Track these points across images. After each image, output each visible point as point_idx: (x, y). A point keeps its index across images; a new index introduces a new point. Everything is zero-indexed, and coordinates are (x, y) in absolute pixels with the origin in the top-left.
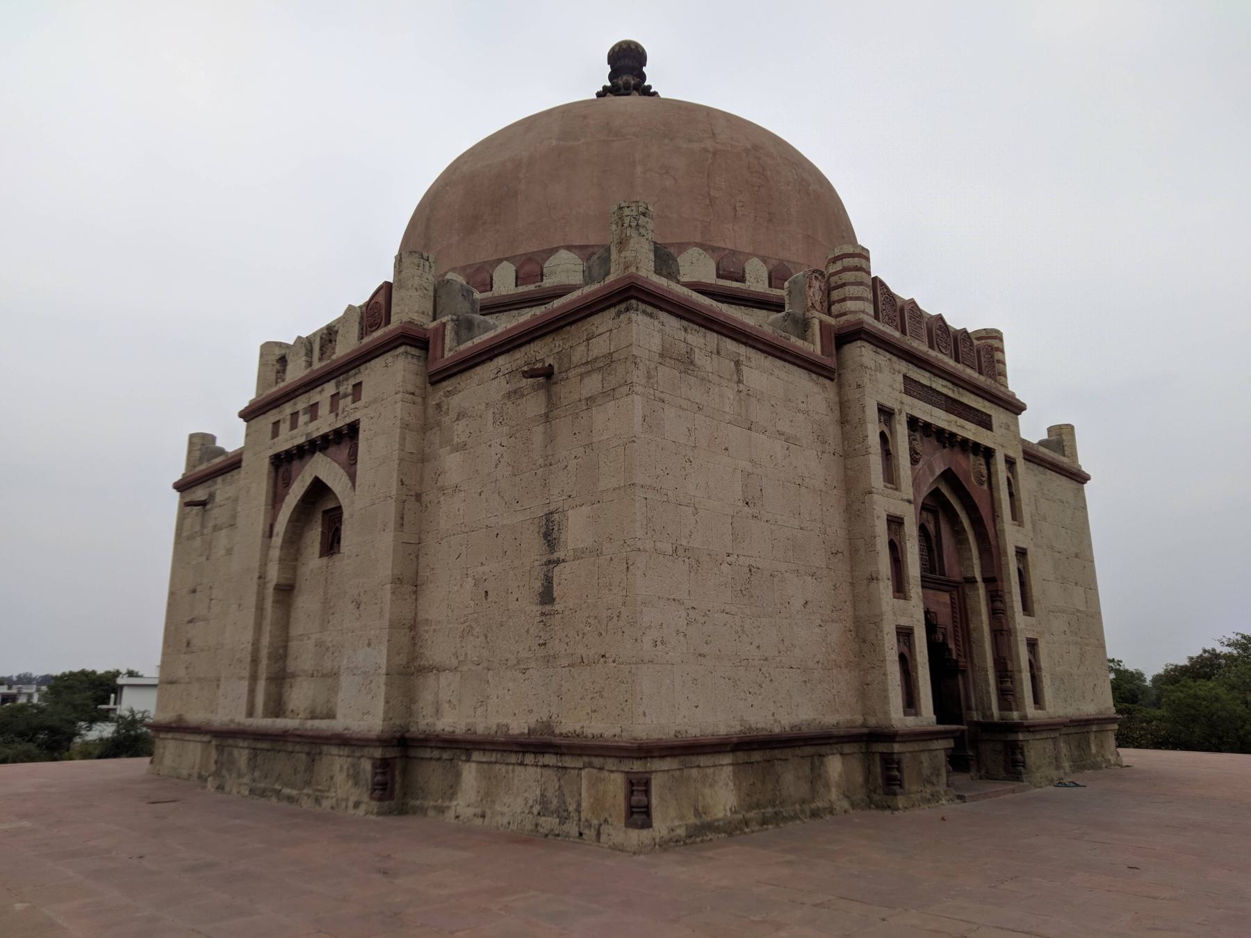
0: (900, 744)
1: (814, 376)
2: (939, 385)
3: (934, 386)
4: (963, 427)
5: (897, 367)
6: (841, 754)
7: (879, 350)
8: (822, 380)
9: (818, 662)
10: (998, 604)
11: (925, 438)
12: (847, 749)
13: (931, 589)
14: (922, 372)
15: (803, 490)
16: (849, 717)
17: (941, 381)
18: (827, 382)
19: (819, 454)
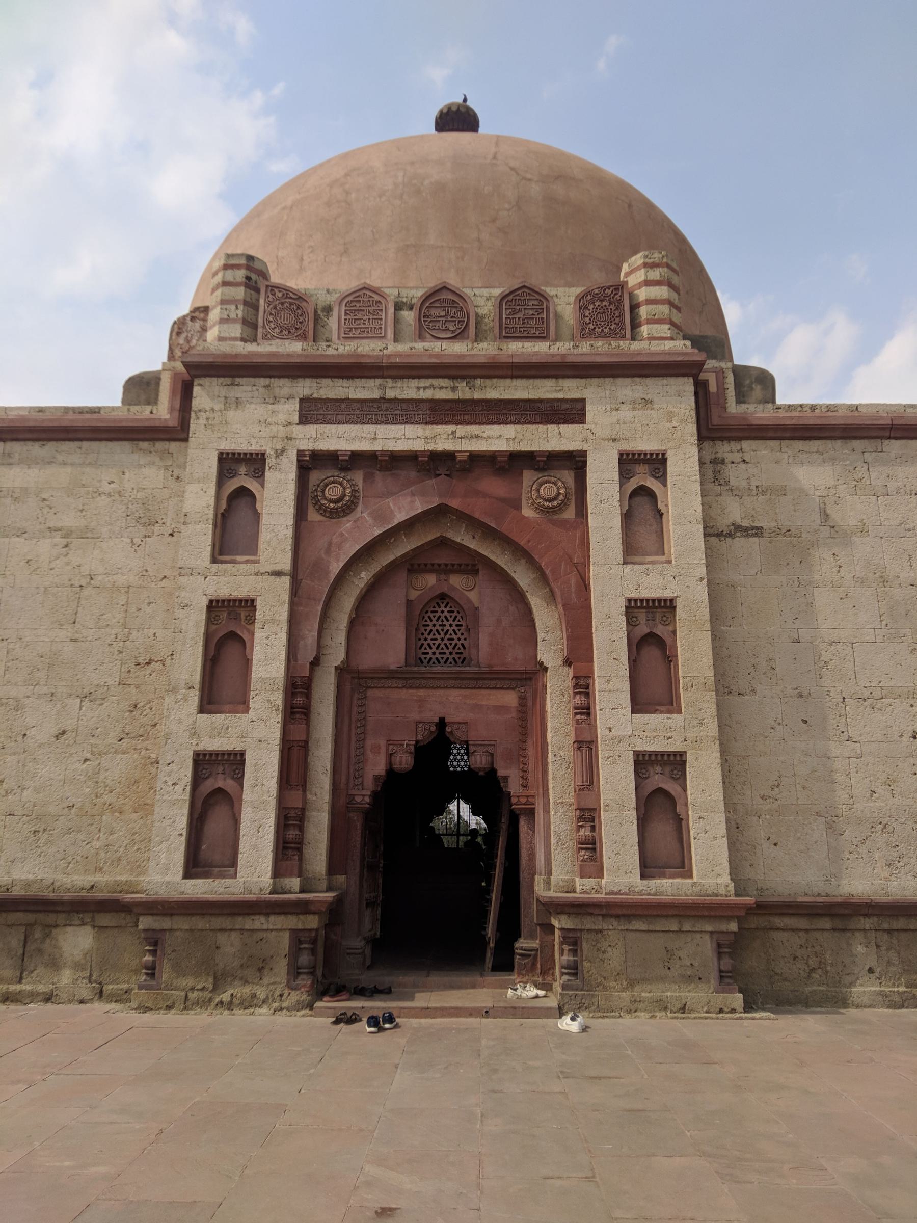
0: (158, 918)
1: (144, 445)
2: (409, 390)
3: (390, 394)
4: (477, 437)
5: (285, 391)
6: (94, 927)
7: (237, 380)
8: (160, 445)
9: (71, 807)
10: (579, 700)
11: (378, 475)
12: (105, 919)
13: (453, 687)
14: (359, 382)
15: (86, 592)
16: (124, 878)
17: (414, 383)
18: (174, 446)
19: (137, 541)
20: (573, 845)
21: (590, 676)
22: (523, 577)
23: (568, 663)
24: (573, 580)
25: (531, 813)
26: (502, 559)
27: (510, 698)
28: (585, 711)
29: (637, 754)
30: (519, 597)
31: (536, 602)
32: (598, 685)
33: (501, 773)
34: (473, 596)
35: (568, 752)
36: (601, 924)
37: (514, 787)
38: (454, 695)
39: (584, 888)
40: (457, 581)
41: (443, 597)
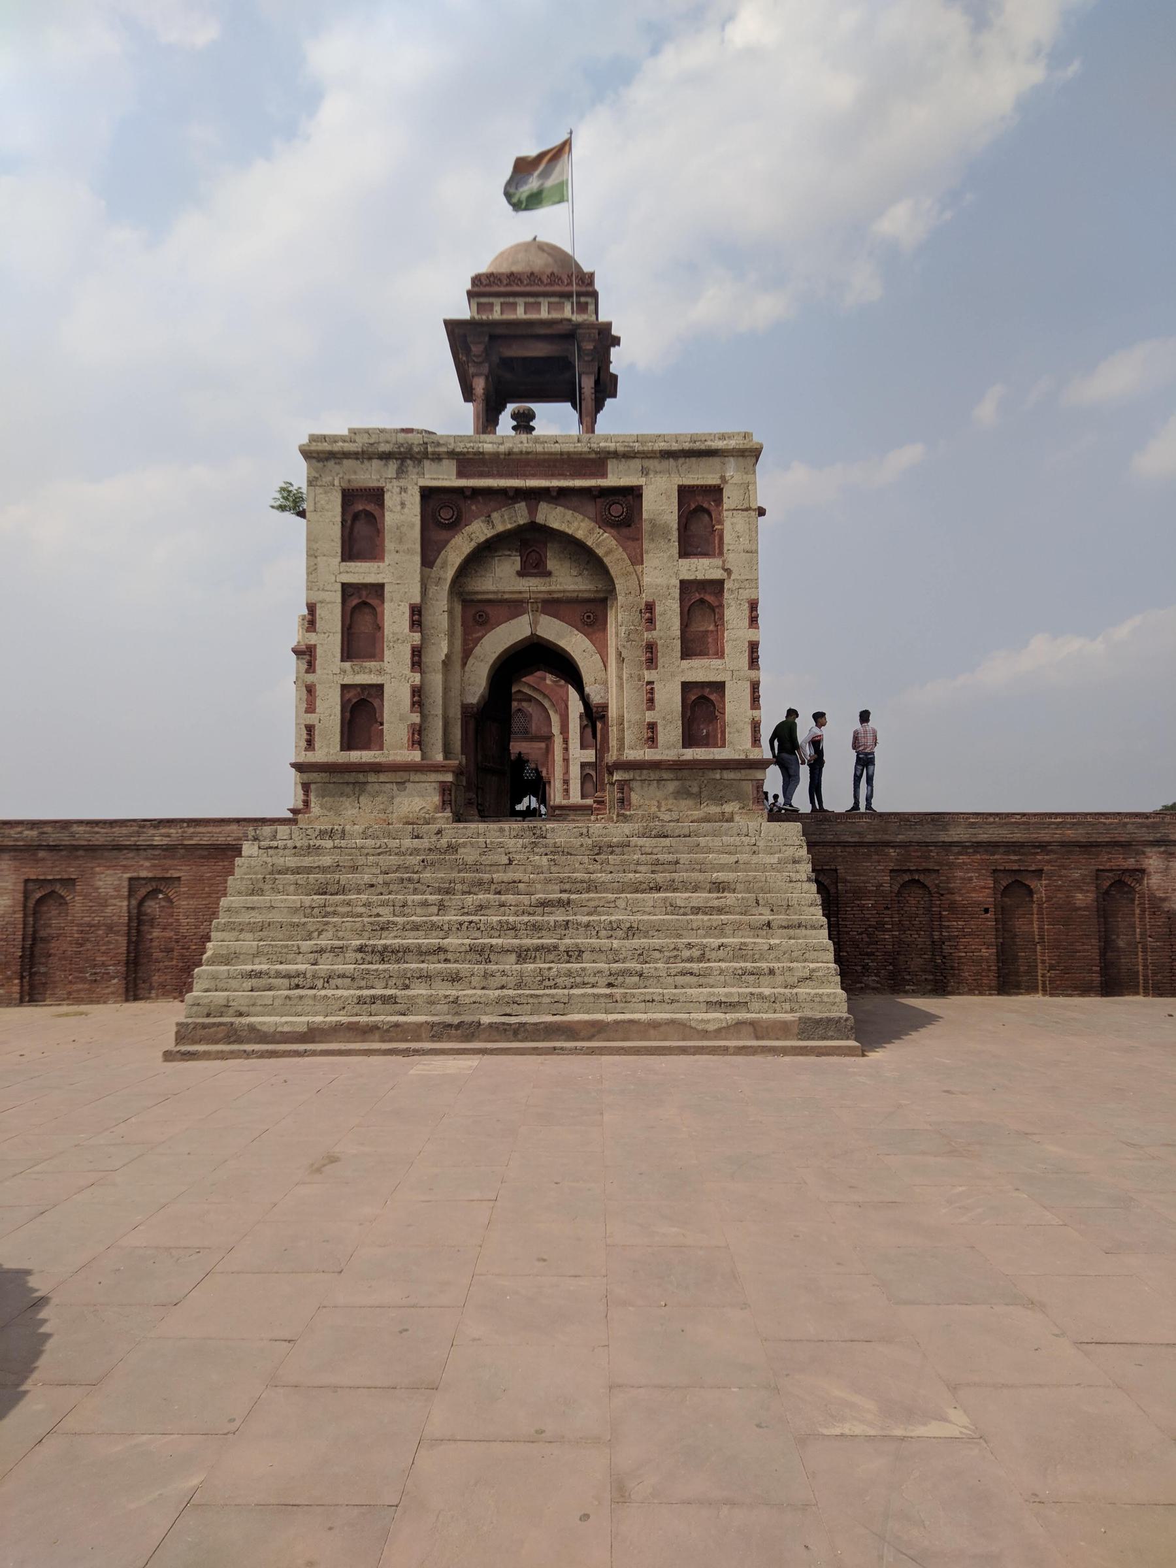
20: (562, 791)
21: (568, 738)
22: (547, 704)
23: (561, 733)
24: (563, 706)
25: (550, 782)
26: (540, 698)
27: (543, 745)
28: (566, 749)
29: (581, 763)
30: (546, 710)
31: (551, 713)
32: (570, 741)
33: (540, 770)
34: (530, 709)
35: (561, 763)
36: (568, 812)
37: (544, 774)
38: (524, 744)
39: (564, 802)
40: (524, 704)
41: (519, 710)
